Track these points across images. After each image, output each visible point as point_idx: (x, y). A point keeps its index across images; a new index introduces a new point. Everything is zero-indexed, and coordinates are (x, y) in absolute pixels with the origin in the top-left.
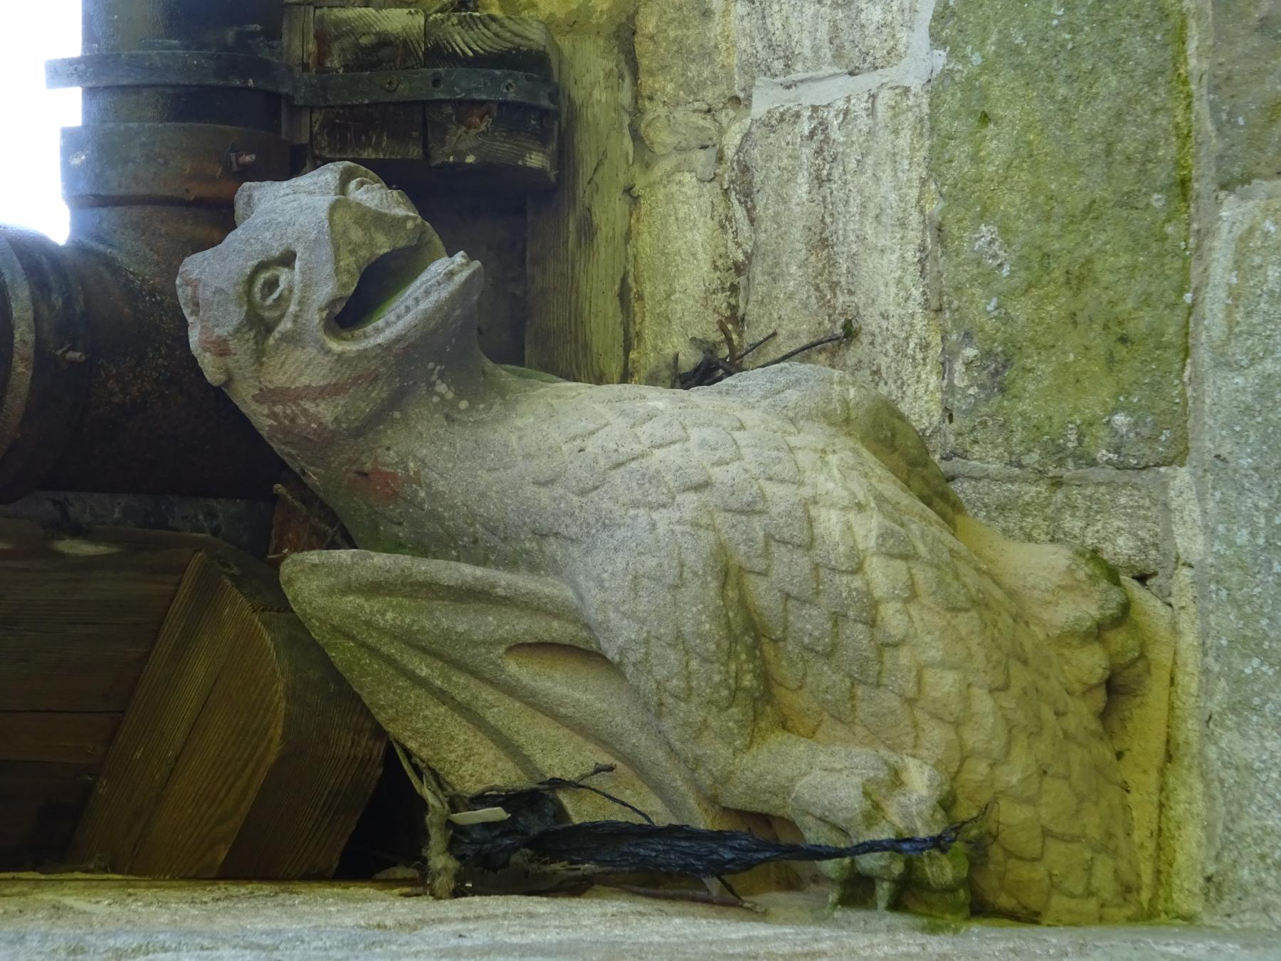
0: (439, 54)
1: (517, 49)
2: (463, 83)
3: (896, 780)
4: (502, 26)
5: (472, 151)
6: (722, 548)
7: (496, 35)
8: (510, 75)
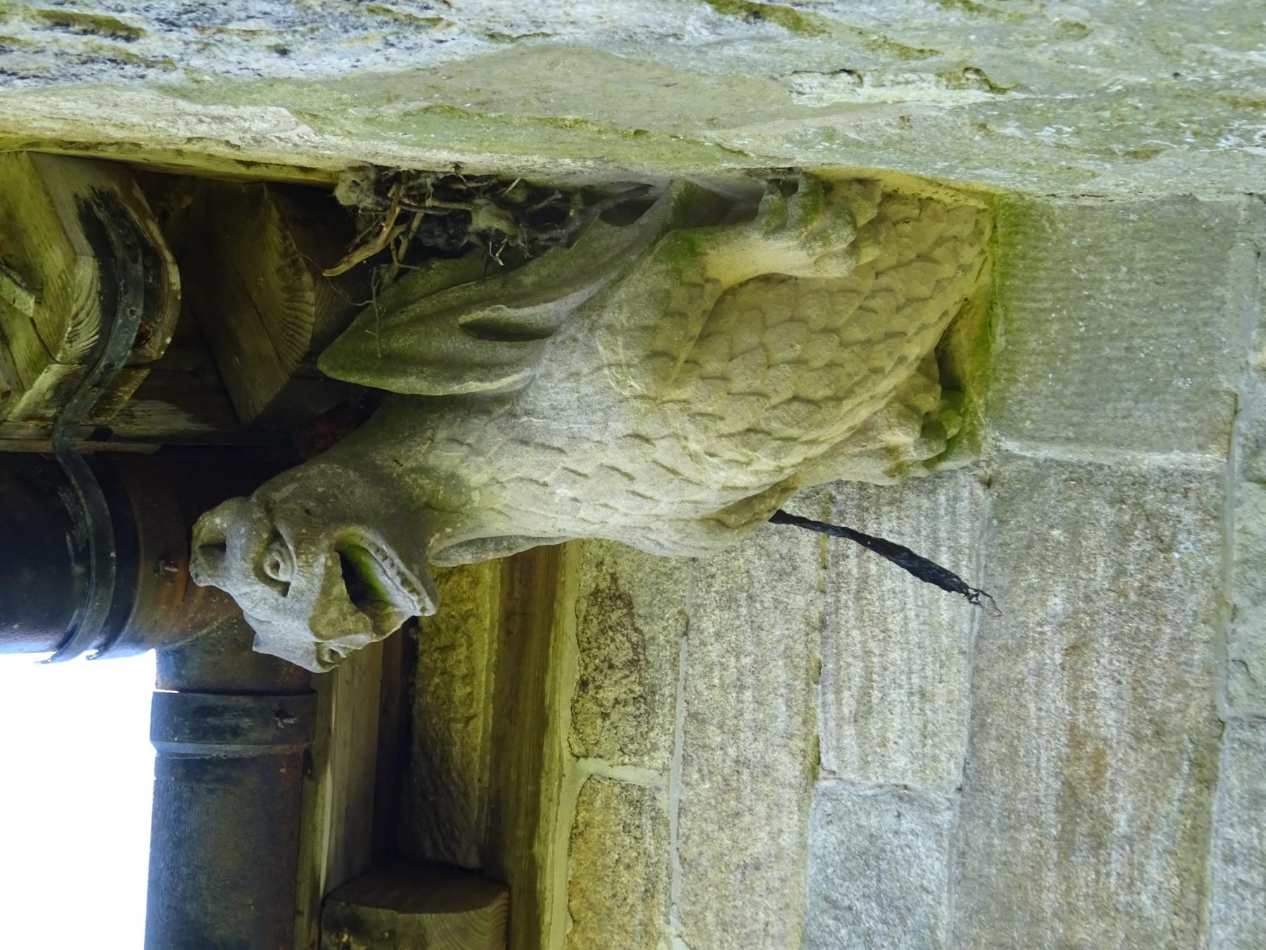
0: (89, 359)
1: (100, 293)
2: (120, 349)
3: (890, 451)
4: (82, 309)
5: (164, 338)
6: (703, 520)
7: (88, 314)
8: (124, 311)
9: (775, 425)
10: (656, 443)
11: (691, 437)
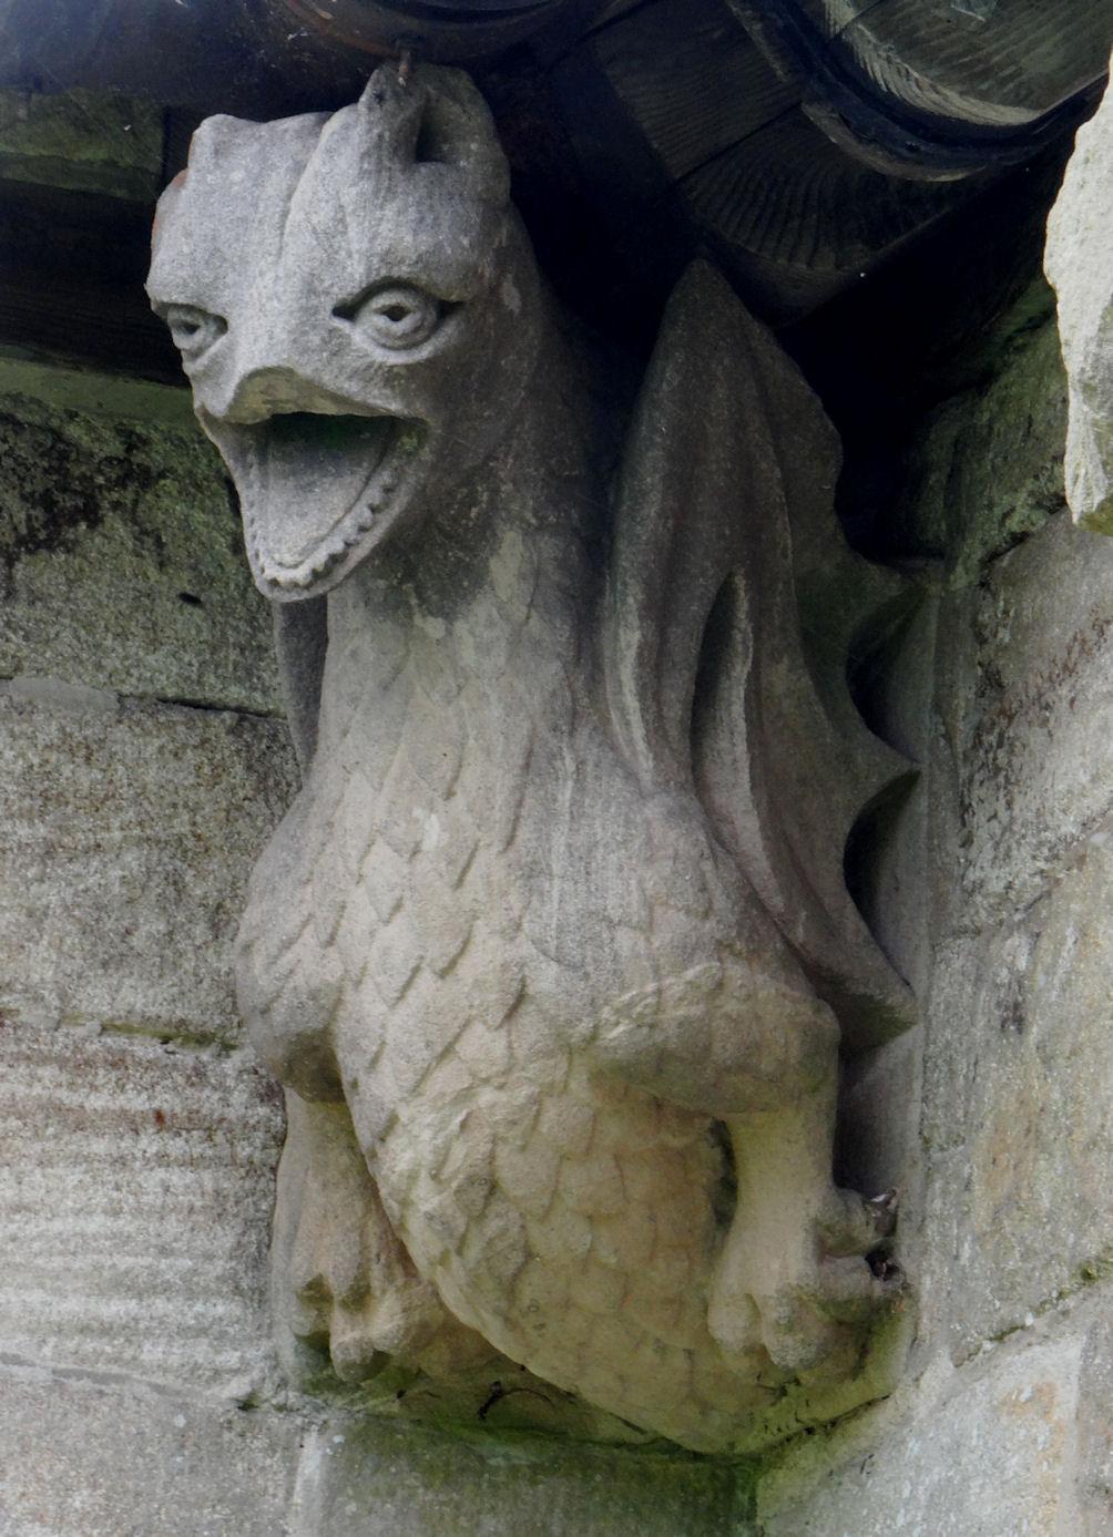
3: (359, 1299)
9: (493, 1226)
10: (503, 1032)
11: (503, 1097)
